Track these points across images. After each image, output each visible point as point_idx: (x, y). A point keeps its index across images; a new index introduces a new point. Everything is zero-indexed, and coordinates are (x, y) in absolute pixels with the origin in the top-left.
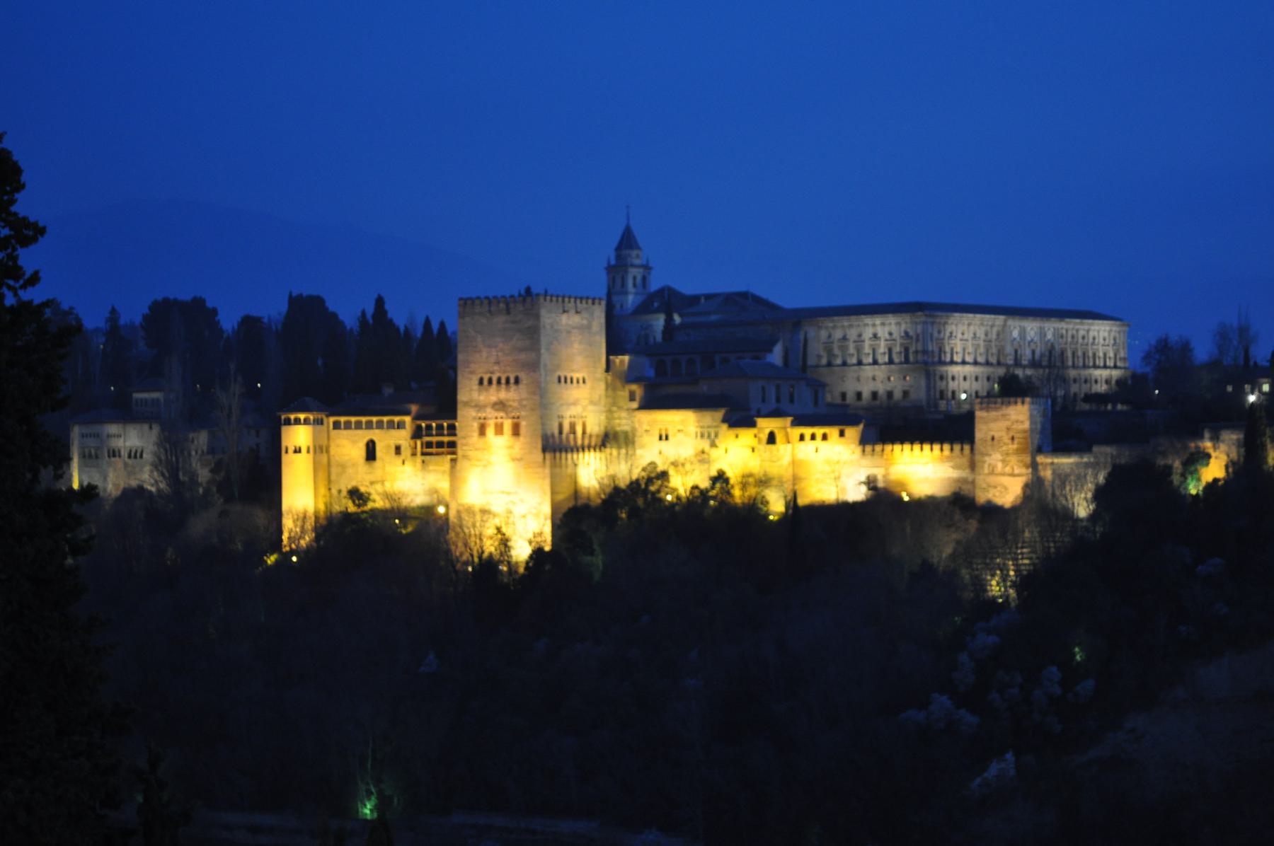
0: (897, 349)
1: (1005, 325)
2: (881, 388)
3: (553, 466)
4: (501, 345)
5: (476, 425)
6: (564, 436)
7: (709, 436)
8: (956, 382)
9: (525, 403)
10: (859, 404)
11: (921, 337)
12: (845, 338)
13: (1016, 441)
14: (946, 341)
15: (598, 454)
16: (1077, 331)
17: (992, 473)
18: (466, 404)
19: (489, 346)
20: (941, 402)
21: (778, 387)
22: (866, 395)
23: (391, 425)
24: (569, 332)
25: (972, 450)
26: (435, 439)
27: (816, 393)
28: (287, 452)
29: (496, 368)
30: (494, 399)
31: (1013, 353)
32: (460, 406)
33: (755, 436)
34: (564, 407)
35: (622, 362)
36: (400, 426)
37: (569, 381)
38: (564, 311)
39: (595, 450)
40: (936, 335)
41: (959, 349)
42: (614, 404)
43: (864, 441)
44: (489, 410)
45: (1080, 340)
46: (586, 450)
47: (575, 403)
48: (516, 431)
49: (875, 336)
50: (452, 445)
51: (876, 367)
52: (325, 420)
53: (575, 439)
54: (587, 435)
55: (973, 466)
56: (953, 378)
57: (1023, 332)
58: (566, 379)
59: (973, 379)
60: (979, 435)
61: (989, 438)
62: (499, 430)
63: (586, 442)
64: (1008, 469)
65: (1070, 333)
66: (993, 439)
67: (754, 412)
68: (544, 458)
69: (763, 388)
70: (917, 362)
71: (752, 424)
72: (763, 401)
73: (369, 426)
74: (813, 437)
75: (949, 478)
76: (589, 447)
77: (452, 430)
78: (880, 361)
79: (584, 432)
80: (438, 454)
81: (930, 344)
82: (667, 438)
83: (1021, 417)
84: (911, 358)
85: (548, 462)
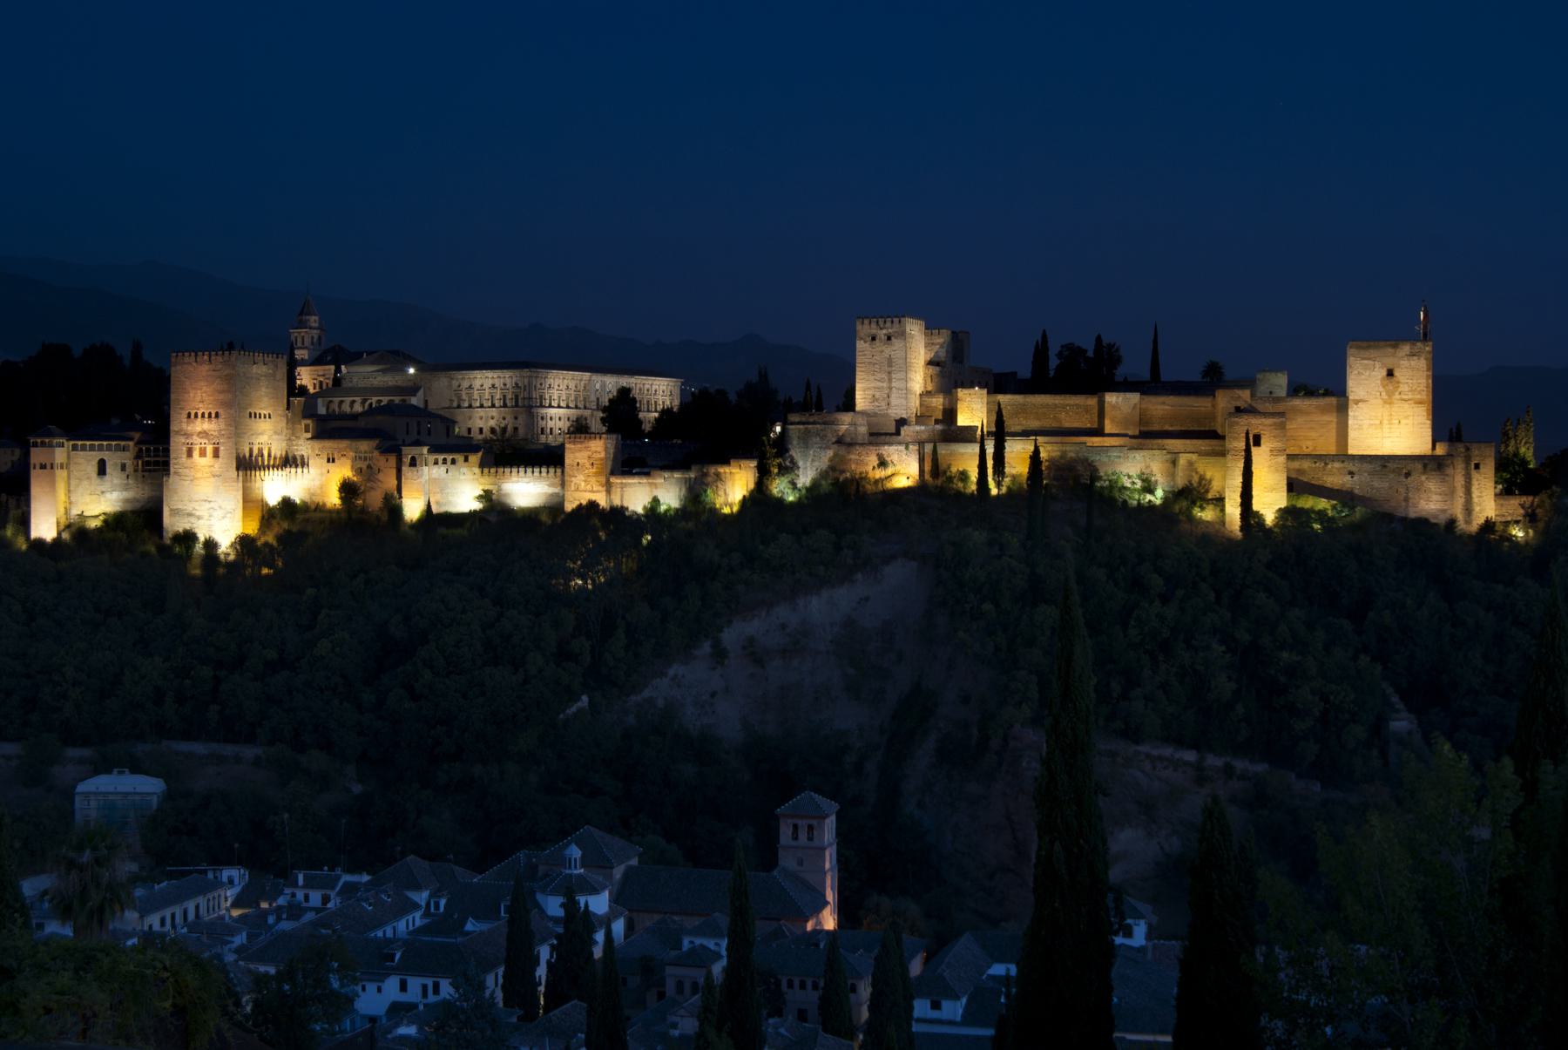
0: (509, 396)
3: (245, 481)
4: (204, 389)
5: (184, 449)
6: (254, 458)
9: (223, 432)
11: (527, 388)
12: (470, 387)
15: (280, 472)
16: (644, 384)
17: (577, 490)
18: (177, 433)
19: (195, 389)
21: (419, 424)
23: (118, 448)
26: (152, 459)
28: (34, 468)
29: (201, 405)
31: (595, 400)
32: (172, 434)
34: (254, 437)
36: (124, 449)
37: (258, 416)
38: (255, 363)
42: (293, 434)
43: (482, 465)
45: (646, 392)
47: (262, 434)
48: (216, 454)
49: (493, 386)
52: (66, 443)
54: (272, 458)
55: (563, 484)
56: (551, 419)
57: (603, 385)
58: (255, 414)
59: (566, 419)
60: (567, 461)
62: (203, 453)
63: (272, 463)
64: (589, 487)
66: (578, 464)
67: (400, 443)
68: (238, 475)
69: (408, 424)
70: (524, 406)
72: (407, 433)
73: (101, 448)
74: (445, 461)
75: (546, 493)
76: (273, 467)
77: (167, 451)
78: (497, 405)
79: (269, 456)
80: (155, 471)
81: (534, 393)
82: (333, 461)
83: (599, 449)
84: (520, 404)
85: (241, 478)
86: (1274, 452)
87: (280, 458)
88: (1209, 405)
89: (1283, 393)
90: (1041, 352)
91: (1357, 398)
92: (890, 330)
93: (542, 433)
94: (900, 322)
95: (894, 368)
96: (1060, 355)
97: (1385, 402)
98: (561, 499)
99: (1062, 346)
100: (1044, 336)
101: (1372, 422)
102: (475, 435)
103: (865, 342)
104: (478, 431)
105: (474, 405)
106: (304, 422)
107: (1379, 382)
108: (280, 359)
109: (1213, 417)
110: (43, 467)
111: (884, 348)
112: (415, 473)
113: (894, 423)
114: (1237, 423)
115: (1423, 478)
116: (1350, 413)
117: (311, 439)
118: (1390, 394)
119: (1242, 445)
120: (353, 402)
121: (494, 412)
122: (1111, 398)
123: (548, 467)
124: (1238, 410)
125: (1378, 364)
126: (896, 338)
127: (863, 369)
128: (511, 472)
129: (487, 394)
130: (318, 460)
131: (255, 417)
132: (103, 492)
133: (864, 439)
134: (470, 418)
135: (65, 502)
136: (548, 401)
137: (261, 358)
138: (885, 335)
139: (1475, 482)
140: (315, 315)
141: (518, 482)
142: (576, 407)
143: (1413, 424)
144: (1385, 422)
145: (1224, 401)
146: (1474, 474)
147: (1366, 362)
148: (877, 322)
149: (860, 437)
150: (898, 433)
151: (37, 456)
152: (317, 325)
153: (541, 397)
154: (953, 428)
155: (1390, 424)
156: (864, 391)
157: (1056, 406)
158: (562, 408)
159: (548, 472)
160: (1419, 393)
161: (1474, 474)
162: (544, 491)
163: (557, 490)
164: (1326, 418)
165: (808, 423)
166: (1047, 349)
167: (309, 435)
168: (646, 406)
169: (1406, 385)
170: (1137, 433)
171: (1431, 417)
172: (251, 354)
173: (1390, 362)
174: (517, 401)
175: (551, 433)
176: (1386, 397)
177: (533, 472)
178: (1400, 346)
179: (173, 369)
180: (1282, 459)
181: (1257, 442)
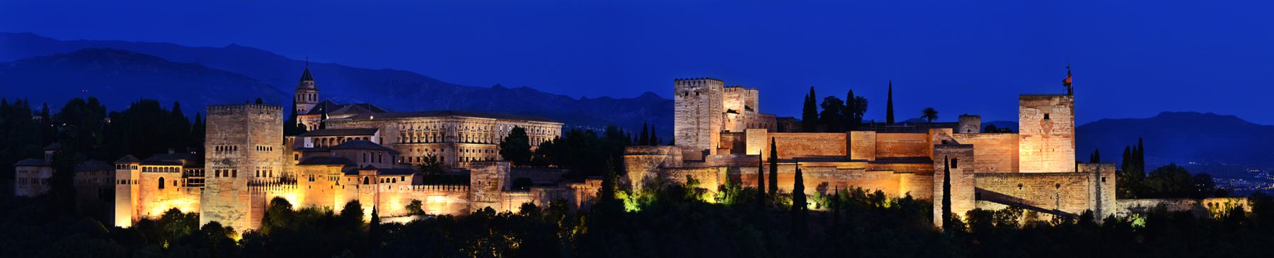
4: (227, 130)
5: (214, 171)
7: (335, 179)
8: (469, 153)
12: (412, 129)
13: (491, 184)
16: (535, 127)
17: (479, 201)
19: (222, 131)
21: (373, 154)
24: (263, 124)
25: (469, 188)
26: (194, 178)
27: (394, 157)
28: (118, 183)
30: (224, 157)
32: (206, 161)
33: (359, 180)
35: (292, 139)
36: (177, 170)
40: (458, 128)
41: (470, 135)
42: (287, 161)
43: (413, 184)
44: (221, 163)
49: (427, 127)
50: (203, 181)
52: (139, 167)
56: (467, 151)
58: (261, 147)
60: (472, 181)
64: (487, 199)
67: (359, 167)
69: (364, 154)
73: (161, 170)
75: (454, 204)
77: (203, 172)
80: (195, 186)
82: (313, 180)
90: (810, 103)
91: (1024, 134)
96: (823, 105)
97: (1043, 137)
99: (825, 99)
100: (812, 91)
103: (681, 97)
106: (294, 153)
107: (1039, 123)
108: (279, 110)
109: (926, 146)
110: (124, 182)
111: (694, 100)
113: (701, 153)
115: (1068, 188)
118: (1047, 131)
120: (332, 139)
121: (425, 146)
122: (854, 135)
125: (1038, 111)
129: (423, 134)
130: (303, 179)
131: (261, 149)
132: (162, 200)
133: (679, 165)
134: (411, 150)
135: (137, 206)
136: (465, 139)
137: (265, 109)
138: (695, 91)
142: (486, 143)
144: (1044, 150)
149: (676, 163)
150: (704, 161)
151: (120, 174)
152: (312, 87)
153: (460, 135)
158: (475, 143)
160: (1066, 130)
161: (1102, 184)
163: (464, 201)
165: (640, 154)
166: (815, 101)
167: (297, 162)
169: (1057, 125)
170: (874, 159)
174: (443, 139)
175: (461, 161)
176: (1044, 133)
177: (449, 189)
179: (207, 117)
181: (954, 166)
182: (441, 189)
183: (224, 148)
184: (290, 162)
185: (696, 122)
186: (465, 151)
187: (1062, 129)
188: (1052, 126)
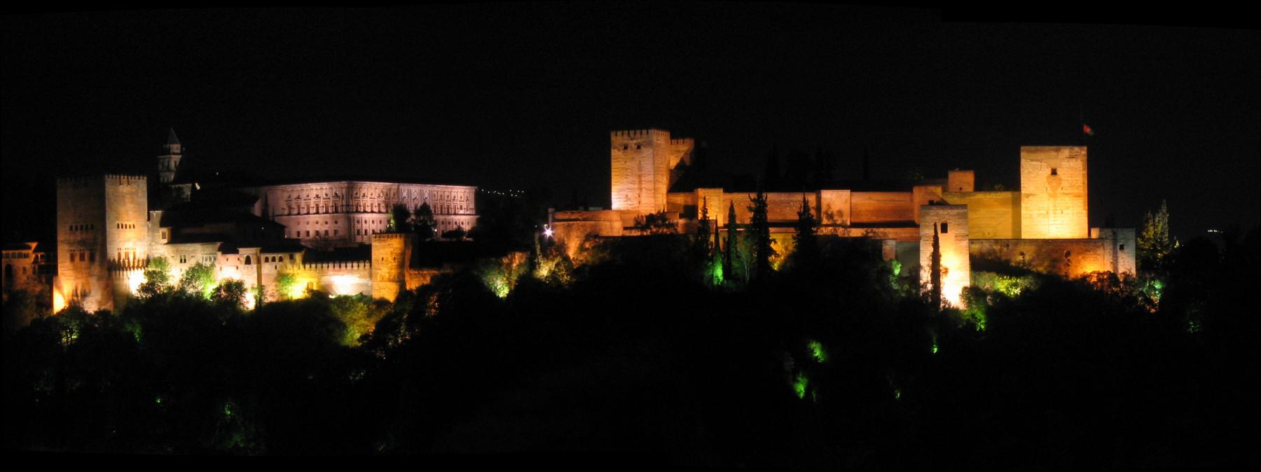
1: (398, 189)
2: (322, 228)
6: (122, 261)
10: (308, 238)
11: (345, 197)
12: (298, 198)
14: (361, 199)
16: (444, 192)
20: (358, 237)
22: (312, 234)
25: (371, 266)
30: (79, 238)
32: (59, 244)
33: (239, 259)
37: (124, 226)
38: (121, 184)
39: (141, 269)
42: (153, 241)
45: (446, 198)
46: (136, 269)
49: (317, 196)
51: (318, 215)
53: (129, 262)
54: (136, 261)
56: (366, 222)
57: (409, 193)
60: (374, 257)
61: (381, 259)
63: (136, 264)
65: (439, 194)
66: (383, 259)
71: (237, 252)
74: (274, 260)
76: (138, 267)
79: (134, 259)
81: (350, 200)
84: (339, 210)
86: (959, 238)
87: (143, 260)
88: (909, 200)
89: (970, 188)
91: (1028, 192)
92: (639, 141)
93: (358, 233)
94: (648, 133)
95: (643, 172)
97: (1050, 196)
98: (369, 289)
101: (1041, 212)
102: (303, 235)
103: (619, 150)
104: (306, 235)
105: (301, 212)
107: (1045, 179)
108: (141, 180)
111: (634, 155)
112: (250, 269)
114: (928, 214)
116: (1023, 205)
117: (166, 244)
119: (932, 232)
123: (334, 263)
124: (932, 203)
126: (644, 146)
127: (617, 174)
128: (328, 267)
131: (122, 227)
134: (299, 223)
137: (126, 180)
138: (635, 144)
139: (1120, 261)
140: (177, 143)
141: (334, 275)
143: (1073, 214)
144: (1051, 212)
145: (919, 195)
146: (1120, 254)
147: (1034, 163)
148: (629, 134)
154: (695, 221)
155: (1055, 213)
156: (619, 192)
157: (782, 202)
158: (375, 213)
159: (358, 266)
160: (1077, 188)
161: (1120, 254)
162: (356, 282)
164: (1002, 209)
168: (440, 210)
171: (1087, 208)
172: (118, 177)
173: (1054, 163)
174: (336, 208)
176: (1051, 192)
177: (346, 266)
178: (1062, 150)
180: (965, 243)
181: (944, 229)
182: (337, 268)
183: (79, 227)
184: (157, 241)
185: (637, 181)
186: (363, 221)
187: (1071, 186)
188: (1060, 184)
